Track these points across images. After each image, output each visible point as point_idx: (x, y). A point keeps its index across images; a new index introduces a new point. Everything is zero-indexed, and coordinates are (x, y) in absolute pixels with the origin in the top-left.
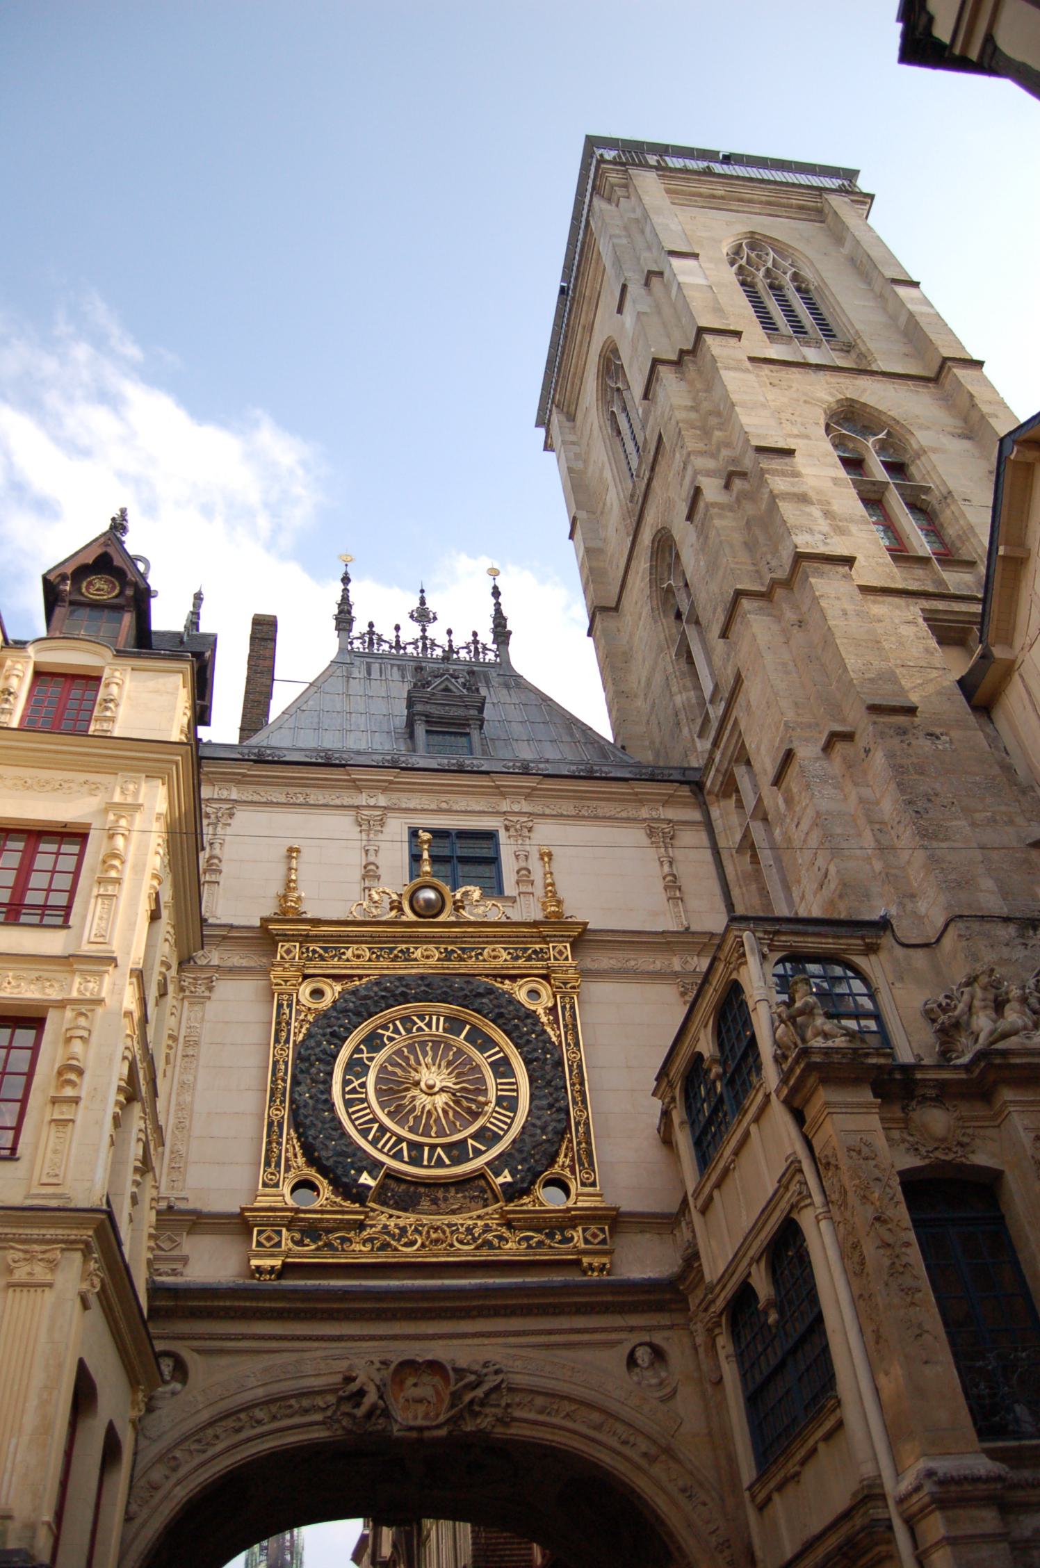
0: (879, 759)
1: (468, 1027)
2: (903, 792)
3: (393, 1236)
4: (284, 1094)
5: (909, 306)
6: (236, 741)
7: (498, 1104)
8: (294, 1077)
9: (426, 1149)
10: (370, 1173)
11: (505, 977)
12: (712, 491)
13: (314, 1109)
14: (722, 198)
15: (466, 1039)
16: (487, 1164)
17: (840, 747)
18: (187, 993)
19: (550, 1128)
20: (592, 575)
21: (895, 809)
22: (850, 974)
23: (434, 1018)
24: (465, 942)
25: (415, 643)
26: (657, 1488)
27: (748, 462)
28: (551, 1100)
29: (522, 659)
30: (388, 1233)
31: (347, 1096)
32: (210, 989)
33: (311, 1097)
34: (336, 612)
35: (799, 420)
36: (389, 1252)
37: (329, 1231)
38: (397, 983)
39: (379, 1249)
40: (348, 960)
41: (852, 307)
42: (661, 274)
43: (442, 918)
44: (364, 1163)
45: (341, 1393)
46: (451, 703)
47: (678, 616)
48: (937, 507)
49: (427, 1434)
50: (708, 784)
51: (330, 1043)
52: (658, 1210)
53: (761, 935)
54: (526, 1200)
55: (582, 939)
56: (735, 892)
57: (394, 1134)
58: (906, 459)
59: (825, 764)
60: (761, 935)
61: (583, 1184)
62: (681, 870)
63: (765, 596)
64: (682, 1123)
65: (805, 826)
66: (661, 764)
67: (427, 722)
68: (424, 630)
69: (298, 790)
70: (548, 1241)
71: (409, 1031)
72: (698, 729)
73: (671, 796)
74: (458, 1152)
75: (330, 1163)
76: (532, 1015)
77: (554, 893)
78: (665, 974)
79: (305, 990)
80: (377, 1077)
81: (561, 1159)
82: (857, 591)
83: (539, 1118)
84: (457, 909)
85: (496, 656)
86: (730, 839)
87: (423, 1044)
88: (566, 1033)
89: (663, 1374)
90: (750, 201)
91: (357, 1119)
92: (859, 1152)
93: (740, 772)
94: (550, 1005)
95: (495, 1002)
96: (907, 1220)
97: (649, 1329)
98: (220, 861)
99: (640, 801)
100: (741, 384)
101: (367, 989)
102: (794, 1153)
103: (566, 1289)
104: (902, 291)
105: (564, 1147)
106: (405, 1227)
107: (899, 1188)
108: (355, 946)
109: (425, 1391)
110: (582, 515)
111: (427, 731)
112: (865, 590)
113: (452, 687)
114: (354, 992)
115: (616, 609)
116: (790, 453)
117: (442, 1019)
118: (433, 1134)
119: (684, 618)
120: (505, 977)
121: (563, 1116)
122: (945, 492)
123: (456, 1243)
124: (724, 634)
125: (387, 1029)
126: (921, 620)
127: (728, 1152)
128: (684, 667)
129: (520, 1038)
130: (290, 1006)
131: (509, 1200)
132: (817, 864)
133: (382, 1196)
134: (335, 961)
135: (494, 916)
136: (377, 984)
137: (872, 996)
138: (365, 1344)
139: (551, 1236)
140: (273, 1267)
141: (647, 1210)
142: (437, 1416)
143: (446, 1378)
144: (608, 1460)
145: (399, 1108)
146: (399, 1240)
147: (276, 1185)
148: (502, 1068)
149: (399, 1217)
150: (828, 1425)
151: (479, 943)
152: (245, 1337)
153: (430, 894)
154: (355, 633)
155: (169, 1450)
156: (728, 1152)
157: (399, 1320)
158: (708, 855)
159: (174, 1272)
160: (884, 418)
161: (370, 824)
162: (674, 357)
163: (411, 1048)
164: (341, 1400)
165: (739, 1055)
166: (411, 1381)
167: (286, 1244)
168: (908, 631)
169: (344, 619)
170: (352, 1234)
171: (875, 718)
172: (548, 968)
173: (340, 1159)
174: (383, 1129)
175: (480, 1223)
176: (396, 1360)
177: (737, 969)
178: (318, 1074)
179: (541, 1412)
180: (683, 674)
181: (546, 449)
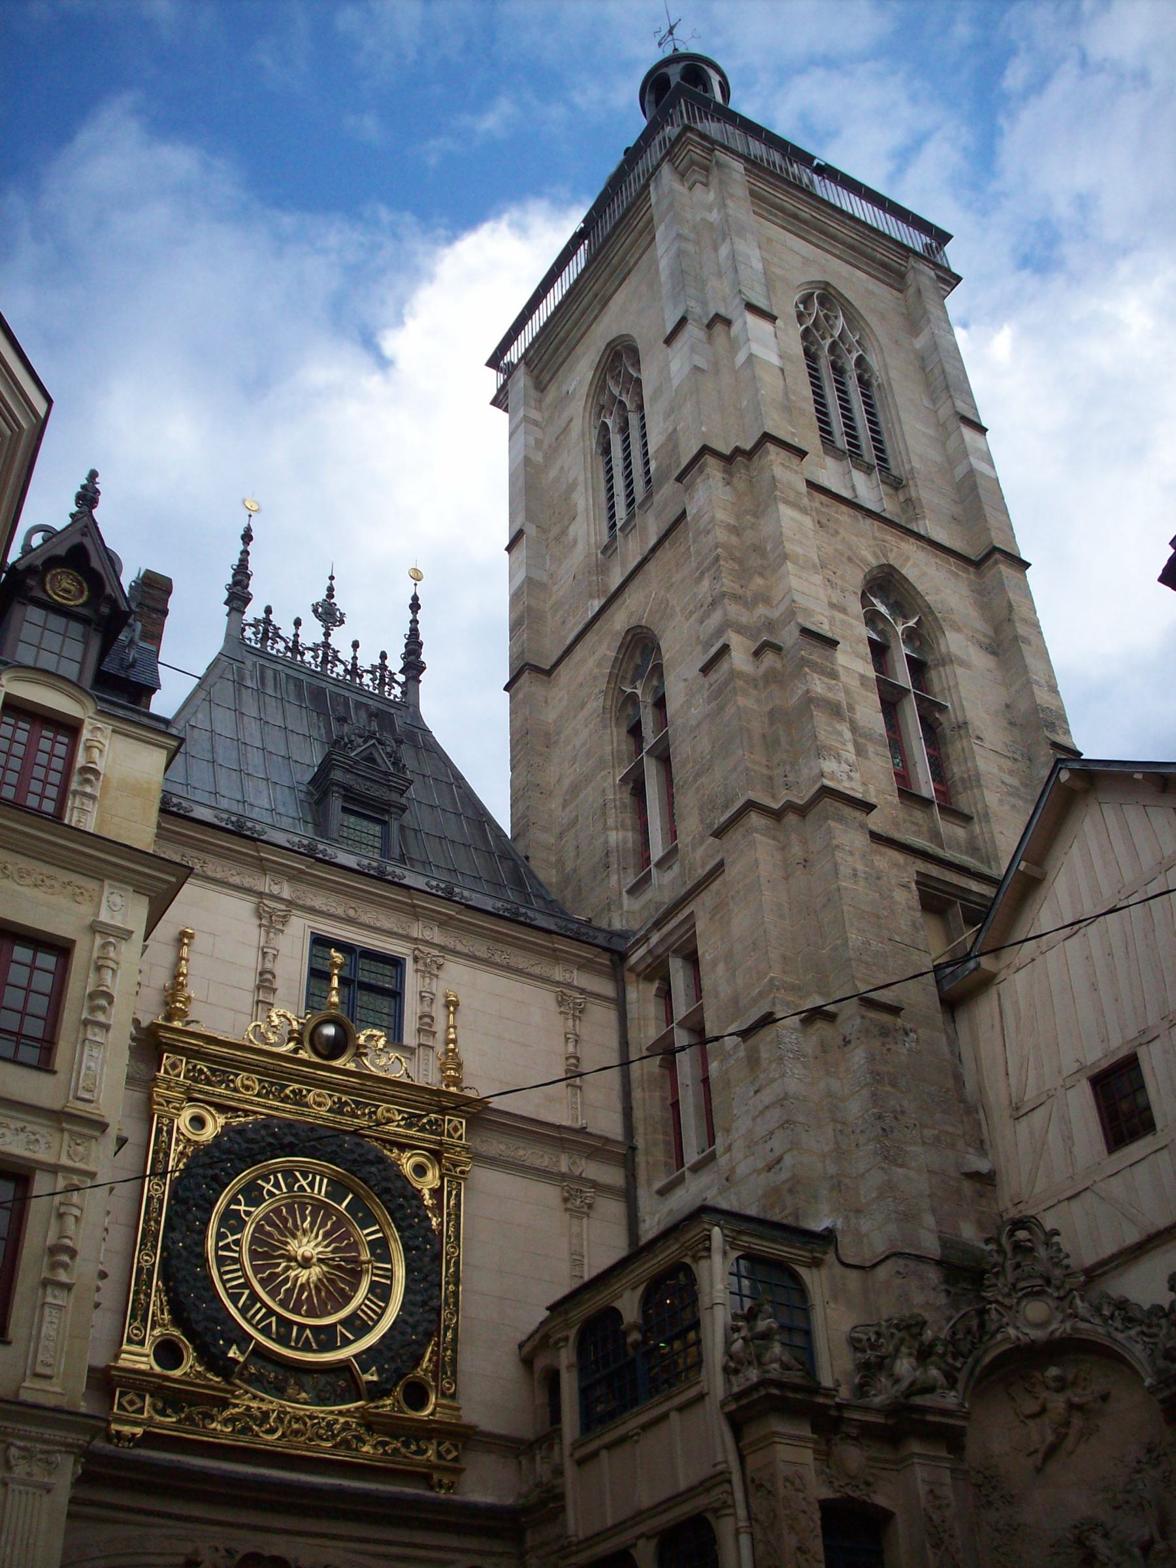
0: (858, 1056)
1: (350, 1196)
3: (254, 1418)
5: (973, 460)
12: (740, 658)
14: (805, 222)
15: (347, 1208)
16: (355, 1356)
17: (820, 1025)
19: (421, 1329)
23: (318, 1178)
27: (788, 636)
28: (425, 1297)
31: (220, 1253)
33: (184, 1247)
34: (230, 581)
35: (839, 582)
36: (247, 1438)
38: (286, 1131)
40: (236, 1090)
41: (914, 437)
42: (728, 323)
44: (232, 1335)
48: (948, 732)
50: (634, 959)
56: (637, 1094)
57: (264, 1304)
58: (930, 659)
60: (726, 1232)
61: (444, 1395)
63: (777, 815)
64: (569, 1367)
65: (767, 1096)
67: (344, 796)
68: (327, 635)
70: (403, 1450)
71: (290, 1188)
74: (327, 1338)
75: (199, 1328)
76: (417, 1195)
81: (425, 1364)
88: (448, 1223)
90: (833, 237)
92: (792, 1483)
95: (384, 1173)
99: (556, 957)
100: (793, 523)
101: (255, 1130)
102: (726, 1462)
103: (415, 1503)
104: (968, 433)
107: (819, 1522)
110: (531, 530)
113: (376, 756)
114: (241, 1130)
115: (548, 673)
116: (832, 643)
117: (325, 1181)
122: (960, 719)
126: (913, 885)
127: (633, 1424)
128: (627, 798)
129: (402, 1219)
130: (170, 1133)
131: (372, 1400)
136: (266, 1127)
137: (805, 1309)
139: (406, 1444)
140: (134, 1435)
147: (141, 1343)
148: (380, 1249)
149: (262, 1400)
160: (919, 601)
161: (271, 920)
162: (727, 451)
163: (290, 1207)
168: (900, 896)
169: (238, 596)
171: (864, 1011)
172: (440, 1143)
173: (211, 1325)
174: (254, 1297)
175: (342, 1420)
176: (244, 1549)
177: (696, 1259)
180: (624, 805)
181: (495, 402)
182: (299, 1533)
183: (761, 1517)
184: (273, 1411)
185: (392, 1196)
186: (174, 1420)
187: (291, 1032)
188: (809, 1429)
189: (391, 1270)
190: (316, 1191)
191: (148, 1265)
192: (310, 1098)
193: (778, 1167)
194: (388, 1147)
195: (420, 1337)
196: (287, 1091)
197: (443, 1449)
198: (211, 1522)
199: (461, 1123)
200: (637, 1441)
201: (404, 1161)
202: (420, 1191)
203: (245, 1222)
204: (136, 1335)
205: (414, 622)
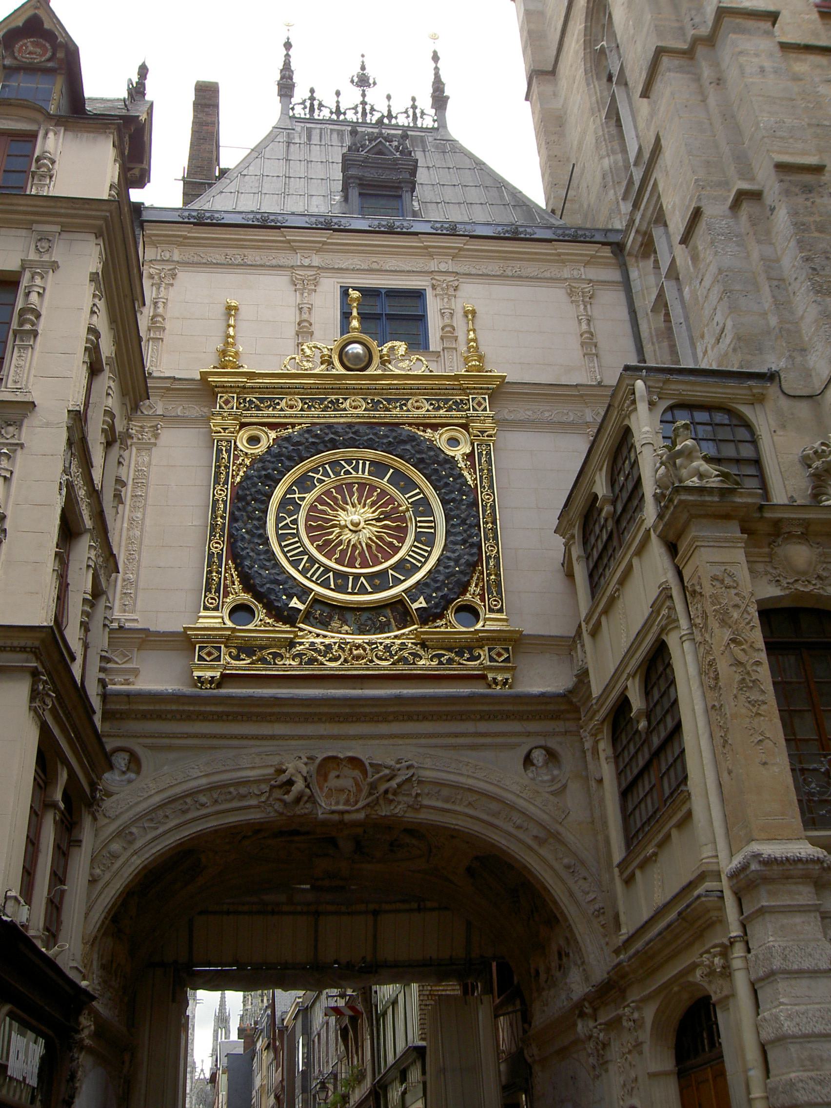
0: (782, 218)
1: (391, 471)
2: (802, 249)
3: (319, 652)
4: (223, 530)
6: (179, 205)
8: (232, 514)
9: (351, 578)
11: (427, 426)
15: (388, 481)
18: (135, 440)
19: (463, 561)
20: (533, 37)
21: (794, 266)
22: (735, 422)
23: (361, 462)
24: (391, 394)
25: (355, 108)
26: (544, 867)
29: (461, 127)
30: (315, 650)
31: (280, 532)
32: (156, 436)
33: (247, 532)
34: (278, 77)
37: (262, 648)
40: (282, 410)
45: (273, 782)
46: (382, 168)
47: (610, 78)
49: (347, 817)
54: (439, 623)
55: (499, 391)
57: (322, 565)
59: (732, 222)
61: (491, 610)
62: (602, 329)
63: (689, 54)
64: (579, 557)
65: (707, 283)
66: (588, 226)
67: (359, 185)
68: (364, 95)
69: (235, 251)
71: (337, 474)
72: (623, 191)
73: (592, 256)
74: (380, 581)
76: (451, 461)
77: (477, 348)
79: (243, 436)
81: (472, 588)
82: (777, 48)
83: (454, 552)
84: (383, 363)
85: (434, 121)
86: (646, 301)
87: (350, 485)
88: (481, 477)
89: (556, 772)
91: (289, 551)
92: (722, 582)
93: (658, 233)
94: (468, 451)
95: (417, 448)
96: (761, 644)
97: (545, 735)
98: (164, 319)
99: (561, 260)
105: (475, 578)
106: (330, 644)
107: (757, 614)
108: (289, 397)
109: (347, 783)
111: (360, 194)
112: (785, 47)
114: (288, 439)
115: (553, 72)
117: (368, 463)
119: (614, 79)
120: (427, 426)
121: (475, 550)
123: (375, 659)
124: (646, 93)
128: (613, 130)
131: (424, 622)
132: (716, 319)
133: (308, 618)
134: (270, 411)
136: (308, 431)
137: (754, 442)
138: (293, 742)
142: (356, 802)
143: (365, 773)
144: (504, 842)
148: (423, 507)
149: (325, 637)
150: (679, 815)
151: (404, 394)
152: (189, 736)
153: (356, 348)
154: (297, 98)
155: (127, 827)
157: (325, 722)
158: (623, 313)
161: (304, 285)
164: (273, 787)
166: (333, 774)
167: (226, 659)
169: (286, 87)
170: (283, 650)
172: (468, 417)
173: (272, 586)
174: (312, 560)
176: (321, 757)
177: (628, 416)
179: (447, 801)
182: (372, 737)
183: (698, 621)
185: (426, 463)
186: (248, 661)
188: (738, 529)
190: (360, 472)
193: (723, 335)
197: (493, 654)
198: (292, 737)
199: (484, 399)
200: (619, 596)
204: (212, 604)
205: (437, 69)
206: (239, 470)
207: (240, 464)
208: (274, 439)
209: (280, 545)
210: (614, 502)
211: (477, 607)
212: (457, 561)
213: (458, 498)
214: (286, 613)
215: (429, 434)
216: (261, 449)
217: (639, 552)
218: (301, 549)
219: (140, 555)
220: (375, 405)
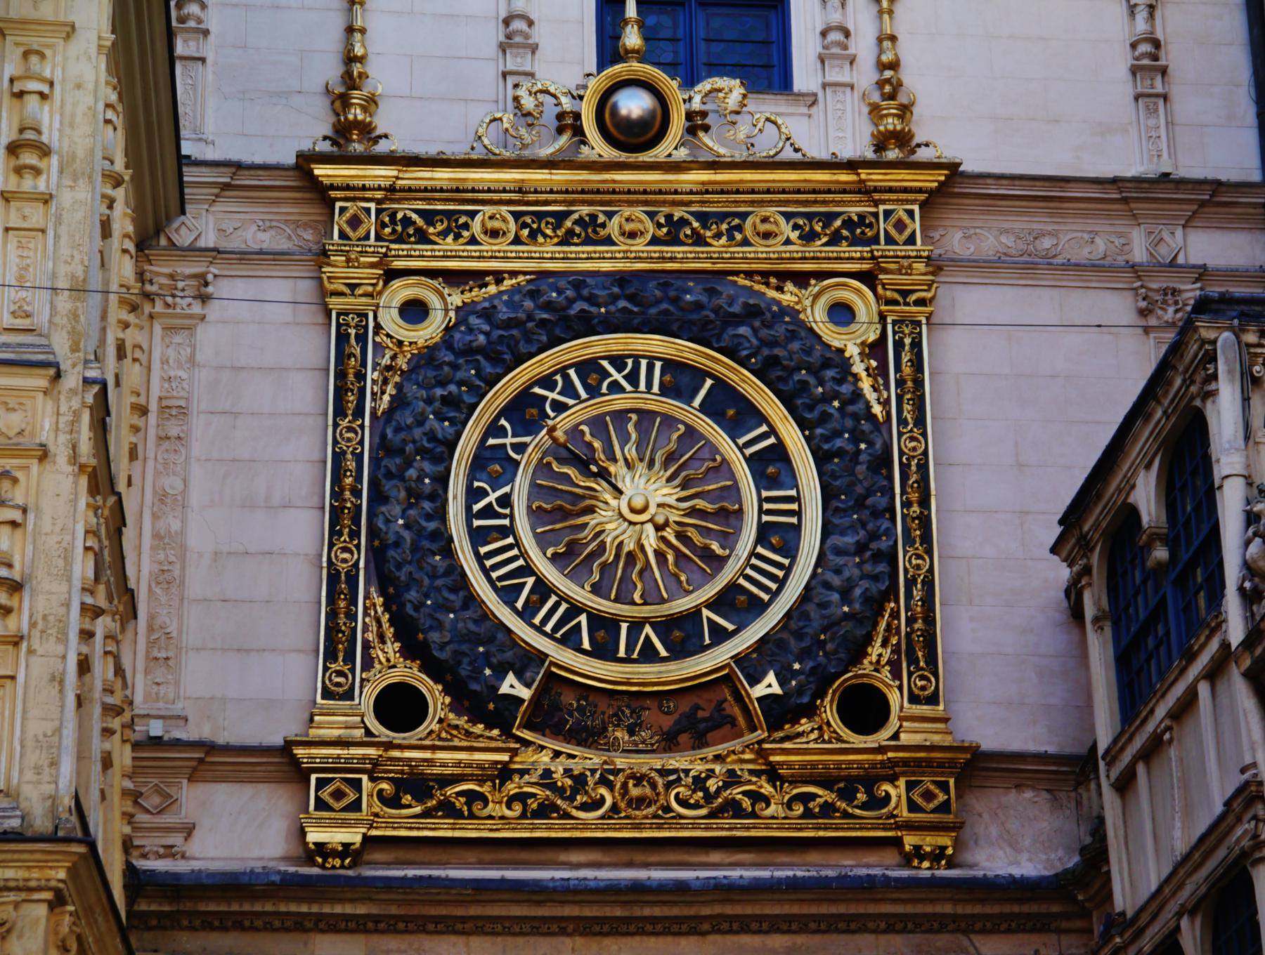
1: (709, 382)
3: (560, 791)
4: (356, 520)
7: (761, 539)
9: (624, 626)
10: (519, 676)
13: (415, 548)
15: (703, 408)
18: (159, 307)
19: (858, 592)
30: (552, 787)
31: (476, 523)
33: (406, 526)
39: (537, 814)
40: (473, 241)
43: (659, 153)
44: (509, 655)
51: (441, 418)
52: (1051, 749)
53: (1251, 338)
54: (805, 725)
57: (563, 598)
60: (1251, 338)
61: (914, 699)
70: (842, 805)
71: (593, 391)
74: (683, 635)
75: (444, 655)
78: (1111, 268)
80: (533, 485)
81: (875, 650)
83: (838, 571)
84: (692, 130)
88: (900, 398)
94: (872, 337)
95: (764, 333)
101: (510, 304)
106: (583, 775)
108: (489, 210)
114: (487, 314)
117: (658, 364)
118: (637, 597)
120: (784, 276)
121: (882, 567)
123: (674, 805)
125: (551, 386)
129: (811, 408)
130: (362, 339)
135: (766, 145)
136: (534, 294)
140: (346, 846)
141: (1032, 747)
145: (573, 548)
146: (571, 799)
147: (349, 695)
148: (771, 465)
149: (573, 757)
156: (1161, 711)
159: (169, 852)
165: (1196, 543)
170: (485, 789)
173: (465, 648)
174: (543, 589)
178: (420, 479)
184: (593, 771)
185: (785, 368)
186: (418, 810)
187: (560, 116)
189: (797, 499)
190: (642, 387)
191: (343, 567)
192: (613, 228)
194: (773, 280)
195: (857, 606)
196: (568, 224)
199: (911, 213)
200: (1171, 741)
201: (808, 303)
202: (841, 351)
203: (517, 463)
204: (338, 685)
206: (385, 381)
207: (389, 368)
208: (458, 309)
209: (477, 554)
210: (1172, 542)
211: (885, 690)
212: (846, 595)
213: (850, 448)
214: (491, 706)
215: (789, 296)
216: (429, 332)
217: (1214, 674)
218: (521, 562)
219: (183, 568)
220: (673, 233)
